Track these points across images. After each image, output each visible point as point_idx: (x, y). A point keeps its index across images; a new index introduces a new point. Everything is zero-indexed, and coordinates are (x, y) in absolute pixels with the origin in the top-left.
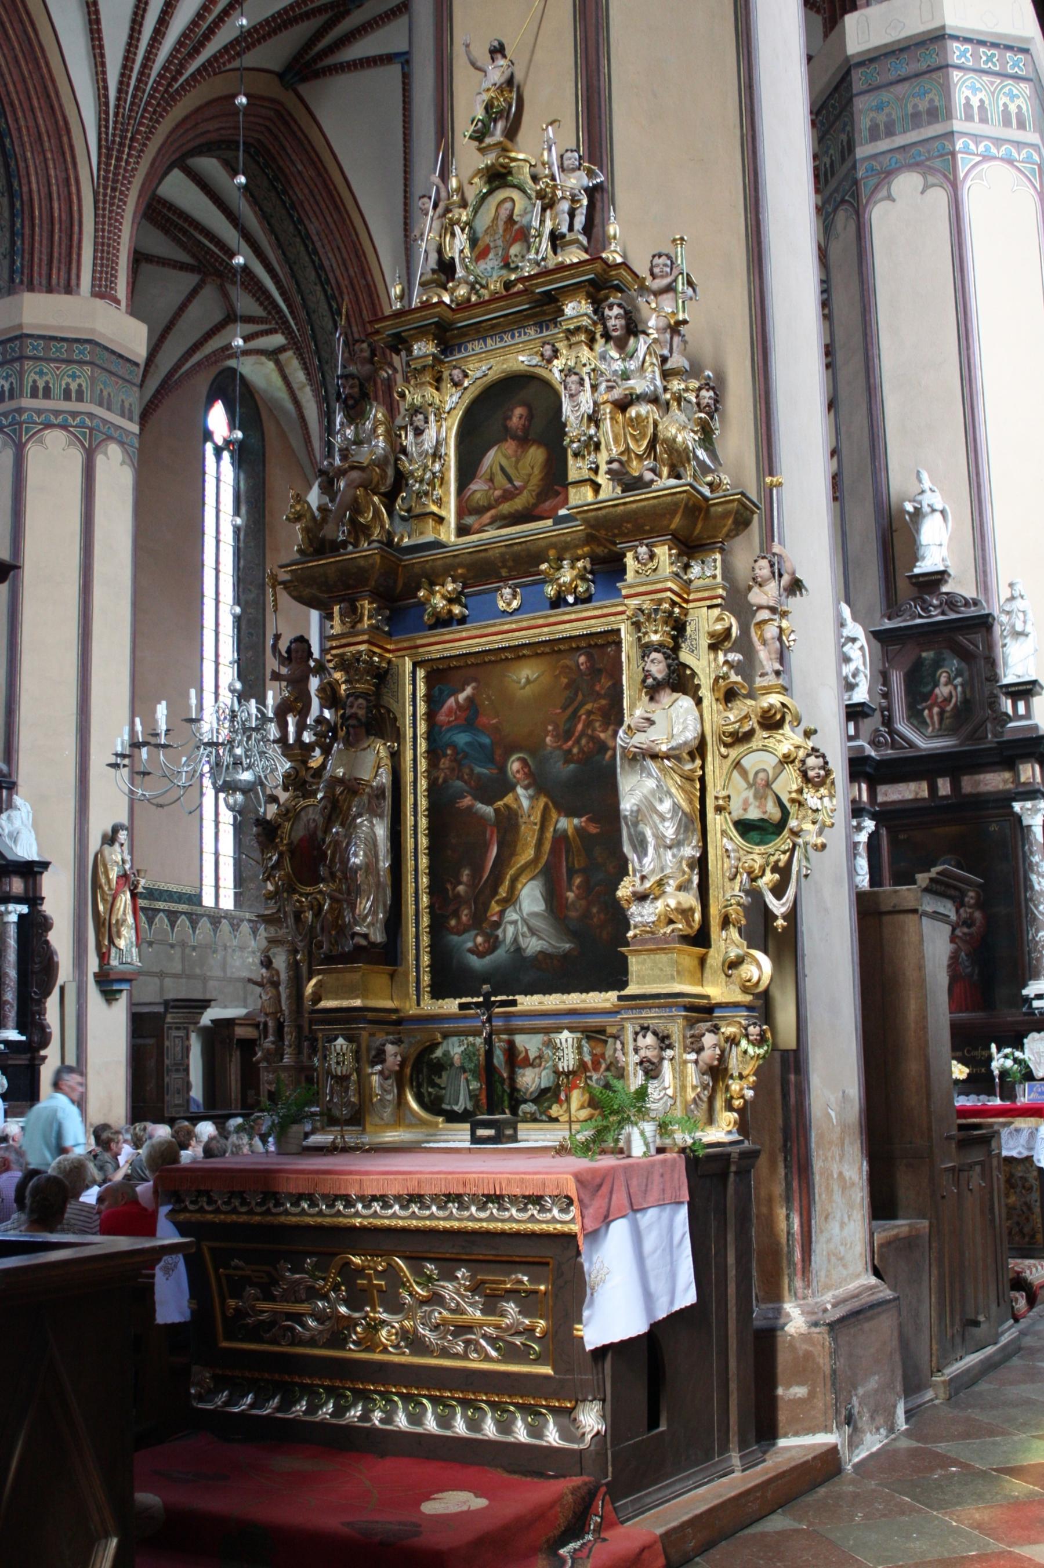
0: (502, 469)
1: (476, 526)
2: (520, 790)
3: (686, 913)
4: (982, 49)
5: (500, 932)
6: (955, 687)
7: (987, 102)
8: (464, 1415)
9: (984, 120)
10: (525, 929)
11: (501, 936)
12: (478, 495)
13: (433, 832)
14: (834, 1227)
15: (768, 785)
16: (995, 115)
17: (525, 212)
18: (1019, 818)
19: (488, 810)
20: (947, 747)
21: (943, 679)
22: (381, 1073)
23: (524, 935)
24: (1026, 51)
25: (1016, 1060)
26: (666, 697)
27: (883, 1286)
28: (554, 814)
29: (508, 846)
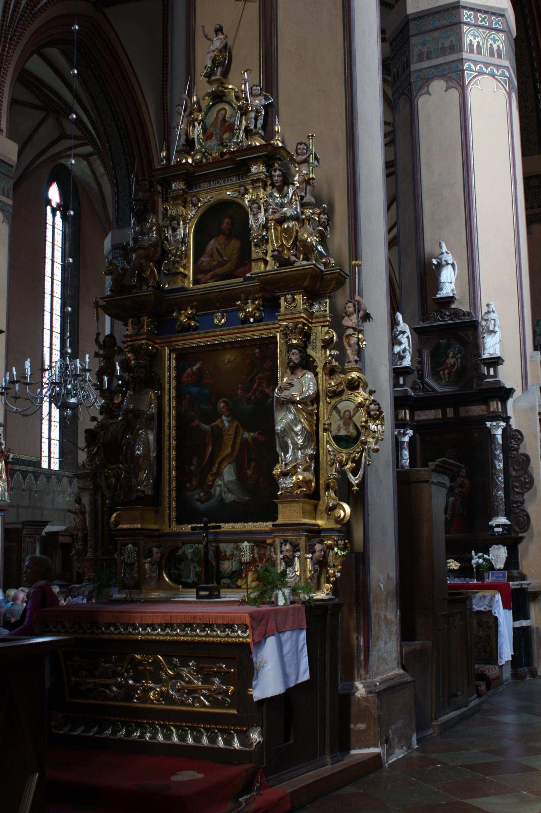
0: (217, 250)
1: (203, 280)
2: (224, 418)
3: (306, 482)
6: (457, 359)
7: (481, 43)
8: (192, 735)
9: (479, 53)
10: (226, 489)
11: (213, 492)
12: (205, 264)
13: (178, 438)
14: (382, 644)
15: (350, 418)
17: (232, 116)
18: (489, 430)
19: (208, 427)
20: (452, 391)
21: (451, 355)
22: (150, 562)
25: (485, 560)
26: (299, 373)
27: (407, 675)
28: (241, 431)
29: (218, 447)
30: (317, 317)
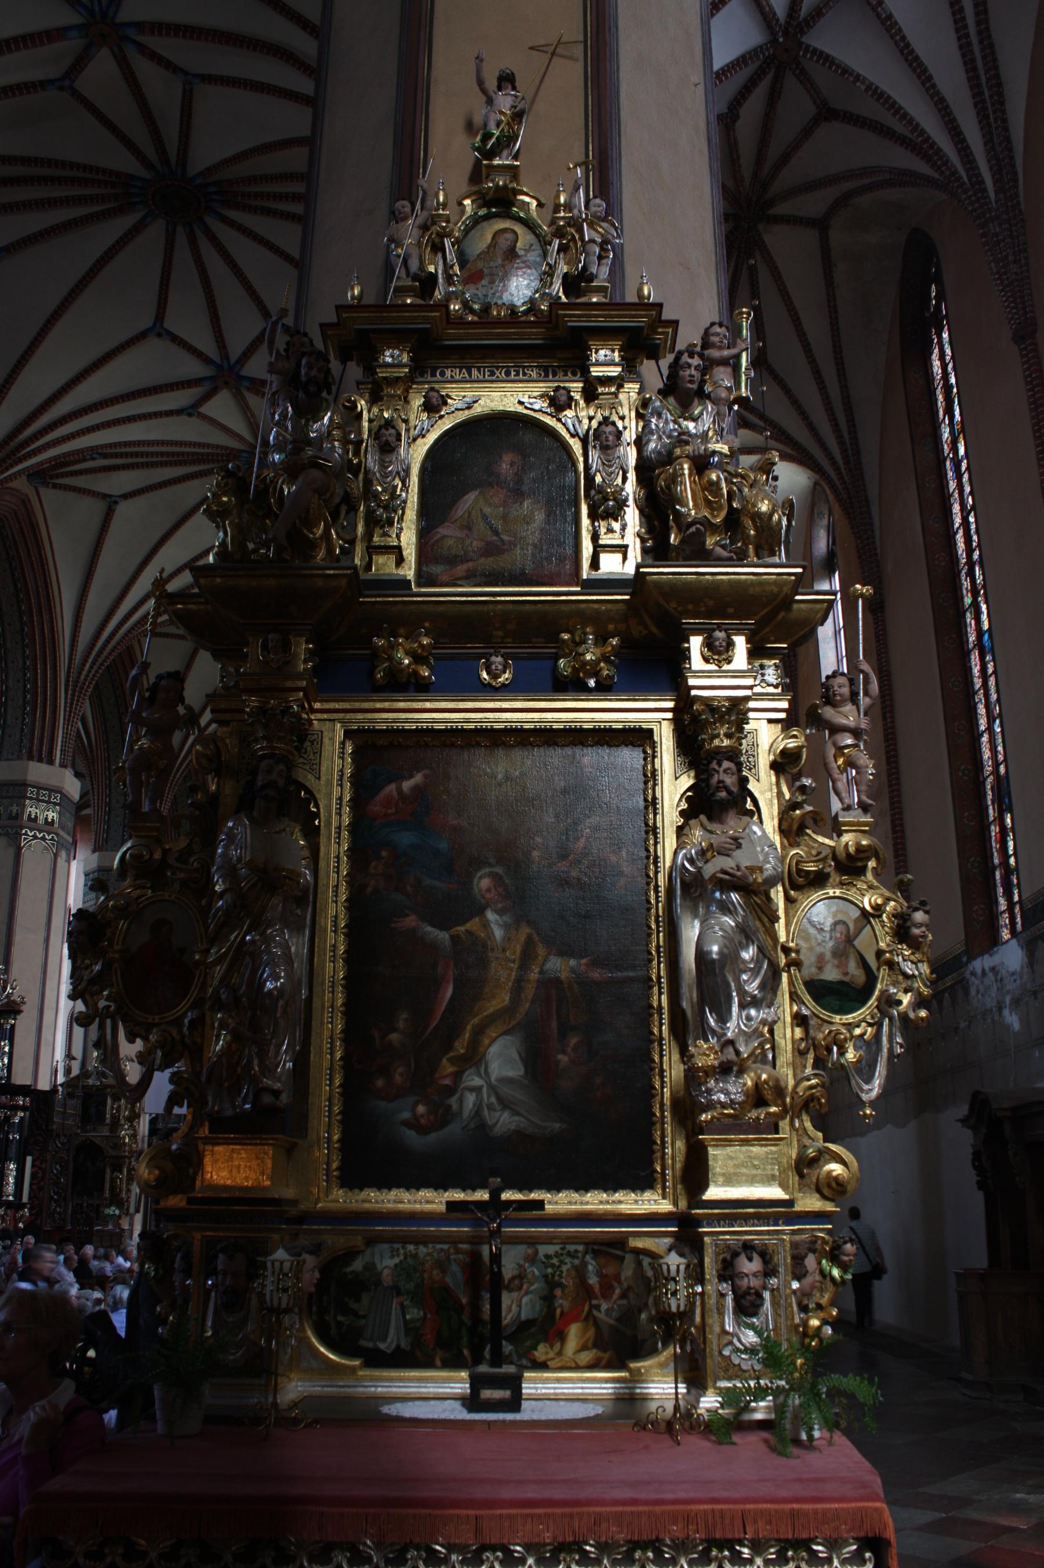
2: (490, 915)
5: (453, 1101)
10: (493, 1099)
11: (455, 1107)
12: (450, 542)
23: (490, 1107)
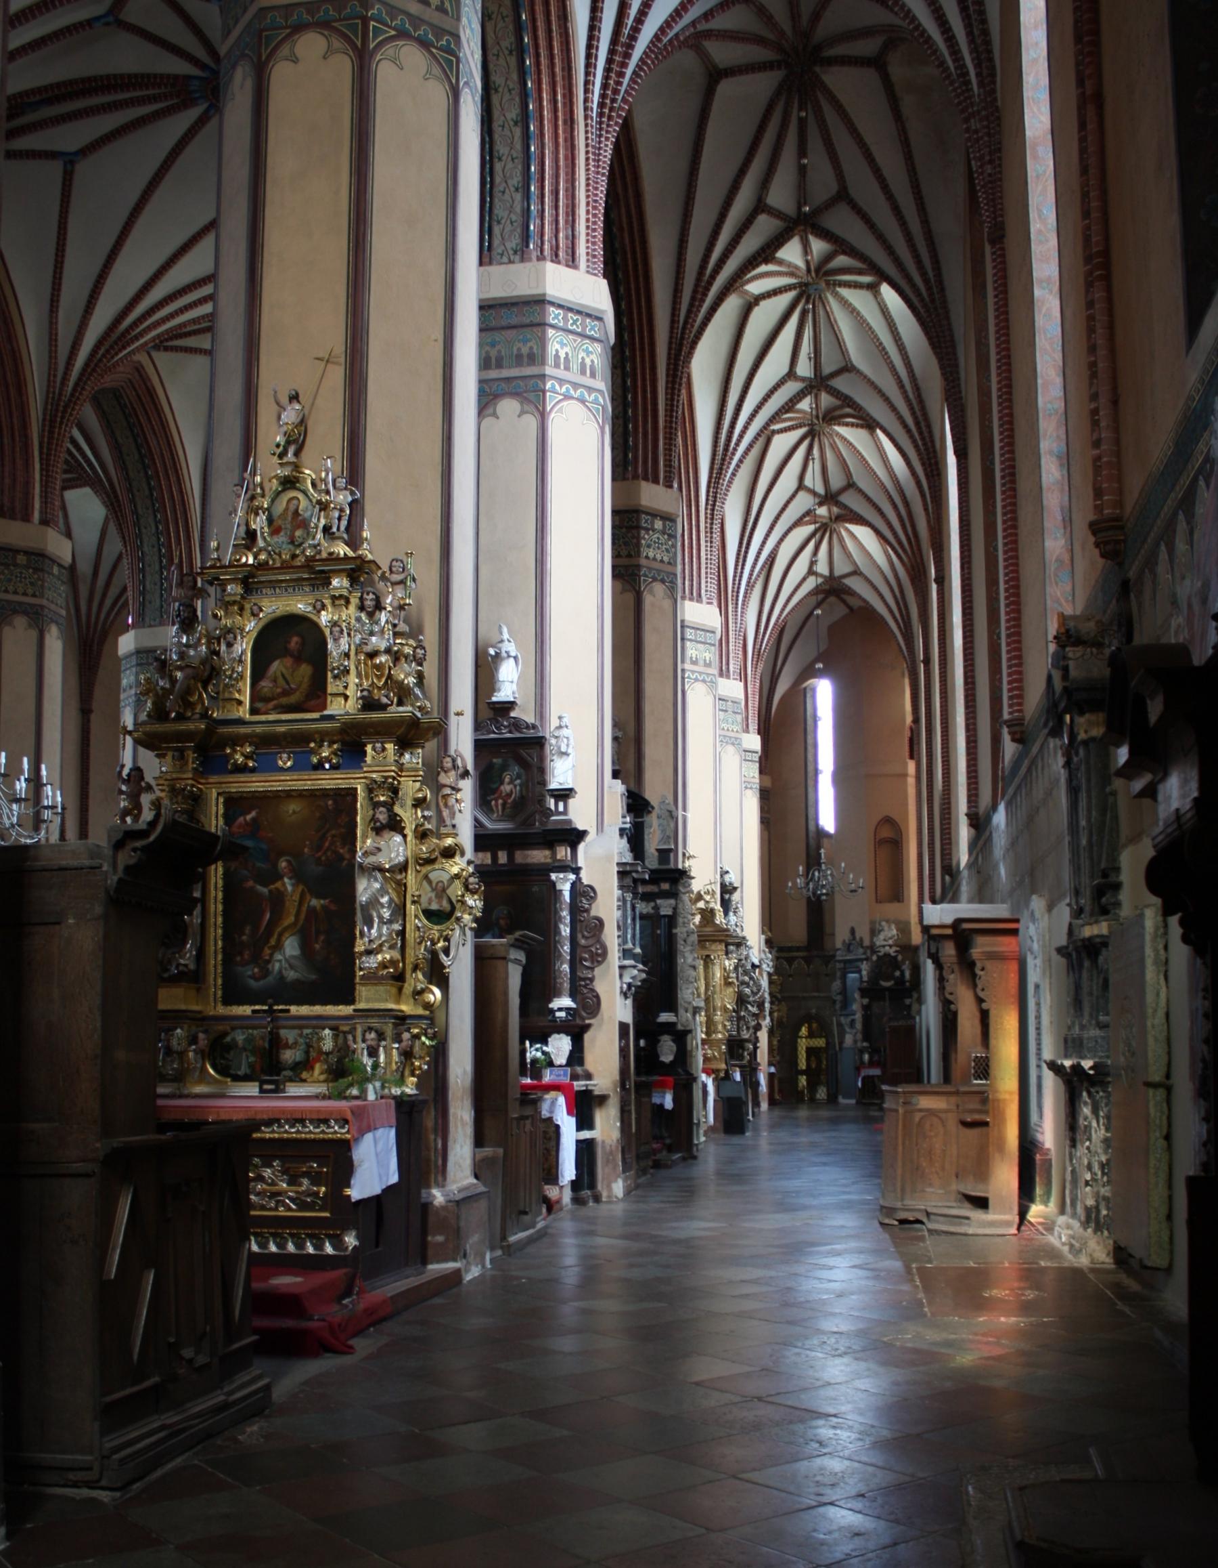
0: (283, 675)
1: (263, 709)
2: (286, 880)
3: (393, 962)
4: (570, 315)
5: (270, 966)
8: (275, 1242)
9: (567, 368)
12: (266, 690)
13: (226, 901)
14: (458, 1147)
15: (444, 890)
16: (575, 367)
17: (306, 510)
18: (554, 884)
19: (265, 890)
21: (507, 780)
22: (194, 1051)
24: (600, 319)
25: (544, 1053)
26: (387, 834)
27: (480, 1184)
28: (308, 896)
29: (277, 914)
30: (408, 770)
